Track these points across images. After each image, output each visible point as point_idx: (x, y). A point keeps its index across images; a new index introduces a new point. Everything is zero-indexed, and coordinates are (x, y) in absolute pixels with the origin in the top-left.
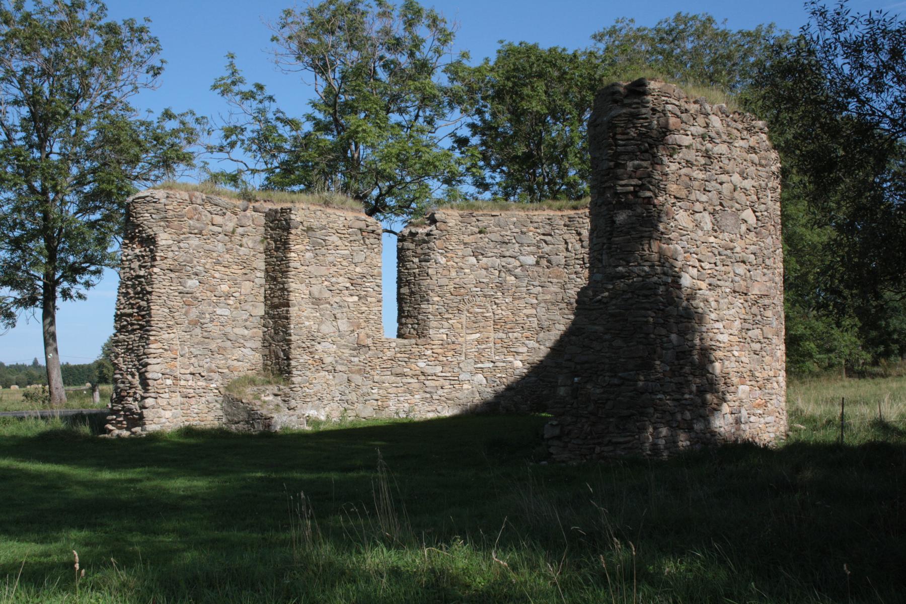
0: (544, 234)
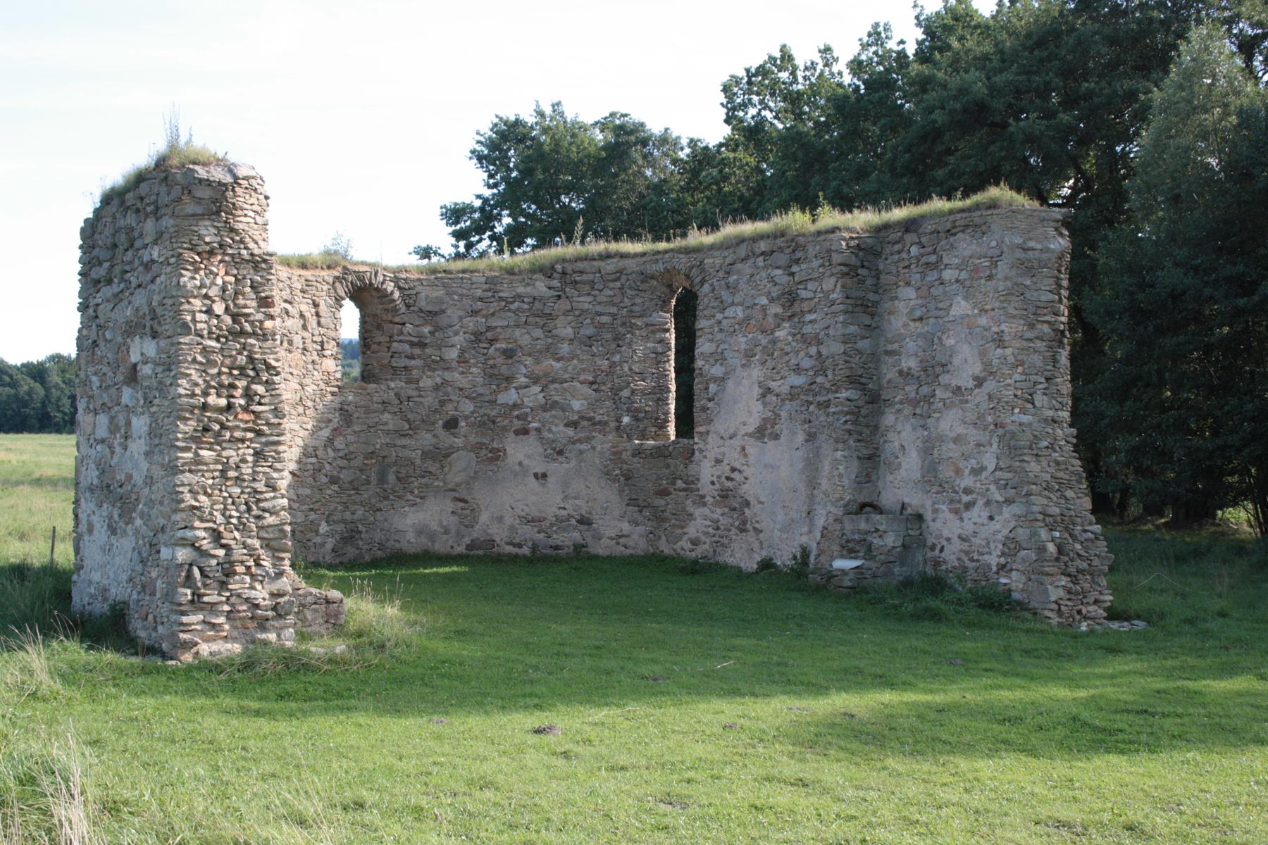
0: (286, 301)
